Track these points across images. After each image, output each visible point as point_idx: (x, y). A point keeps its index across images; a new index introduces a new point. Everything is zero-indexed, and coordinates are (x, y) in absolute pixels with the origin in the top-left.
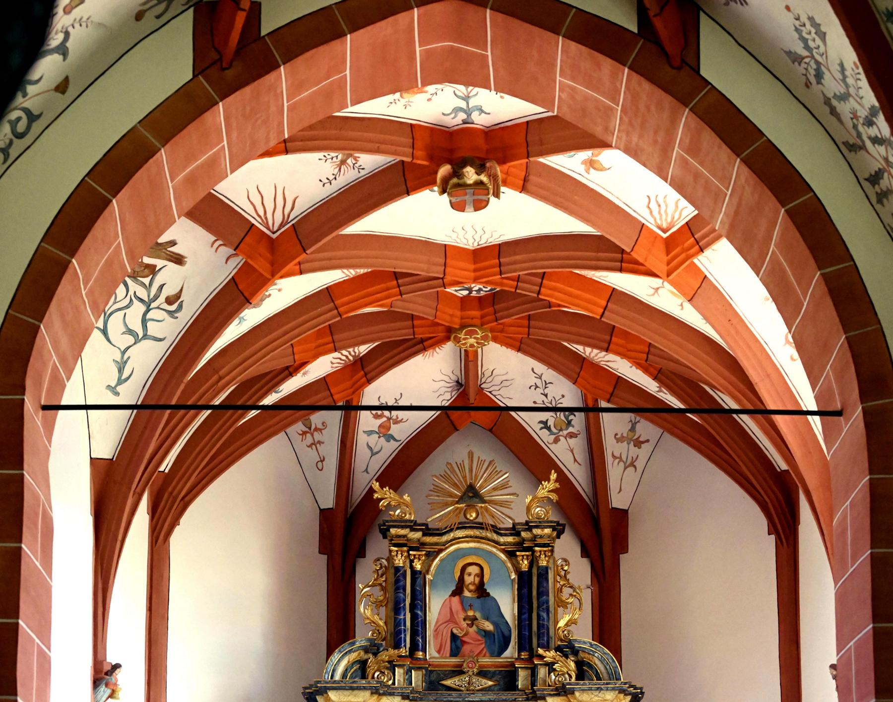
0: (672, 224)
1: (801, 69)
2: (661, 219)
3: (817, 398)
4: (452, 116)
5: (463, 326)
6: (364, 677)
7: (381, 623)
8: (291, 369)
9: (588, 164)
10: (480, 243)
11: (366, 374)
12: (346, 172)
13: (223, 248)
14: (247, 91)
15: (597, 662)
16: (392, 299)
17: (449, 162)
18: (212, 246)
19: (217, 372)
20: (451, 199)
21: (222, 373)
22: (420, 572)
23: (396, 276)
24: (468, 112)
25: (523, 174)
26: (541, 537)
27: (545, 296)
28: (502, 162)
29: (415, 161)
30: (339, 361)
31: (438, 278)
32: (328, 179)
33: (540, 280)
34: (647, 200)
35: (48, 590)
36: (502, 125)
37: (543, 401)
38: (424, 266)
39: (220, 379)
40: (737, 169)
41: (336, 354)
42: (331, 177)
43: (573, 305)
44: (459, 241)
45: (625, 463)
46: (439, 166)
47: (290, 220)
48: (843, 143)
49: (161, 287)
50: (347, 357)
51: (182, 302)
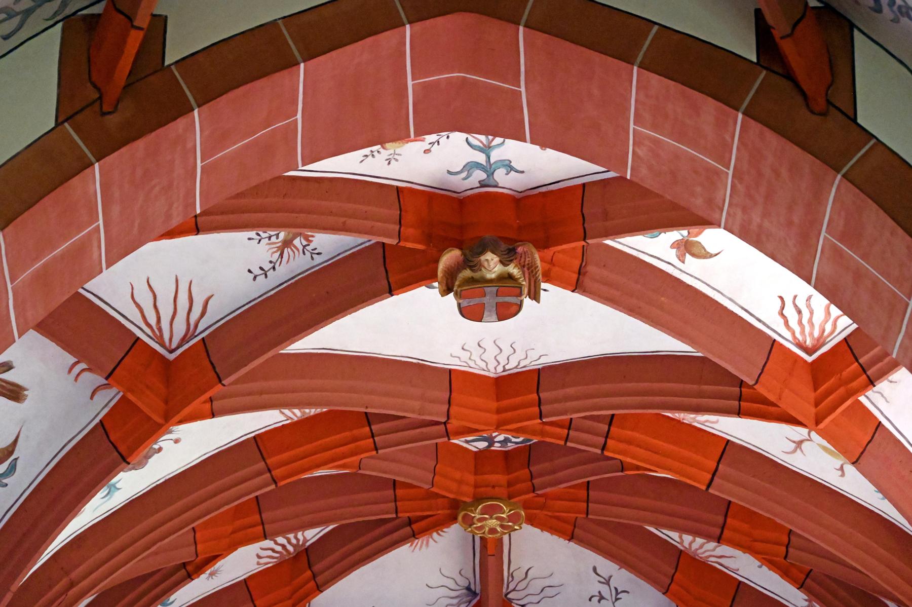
0: (821, 341)
4: (464, 175)
5: (478, 500)
8: (189, 568)
9: (682, 248)
11: (314, 576)
12: (291, 258)
13: (87, 375)
14: (140, 145)
16: (362, 456)
19: (67, 573)
20: (461, 301)
21: (74, 575)
23: (368, 419)
24: (489, 169)
25: (577, 263)
27: (613, 452)
28: (542, 245)
29: (402, 244)
30: (270, 553)
31: (437, 423)
32: (261, 268)
33: (606, 427)
34: (779, 302)
36: (544, 189)
38: (417, 404)
39: (72, 585)
41: (268, 543)
43: (658, 467)
44: (472, 364)
46: (441, 252)
47: (198, 332)
50: (283, 546)
51: (16, 459)
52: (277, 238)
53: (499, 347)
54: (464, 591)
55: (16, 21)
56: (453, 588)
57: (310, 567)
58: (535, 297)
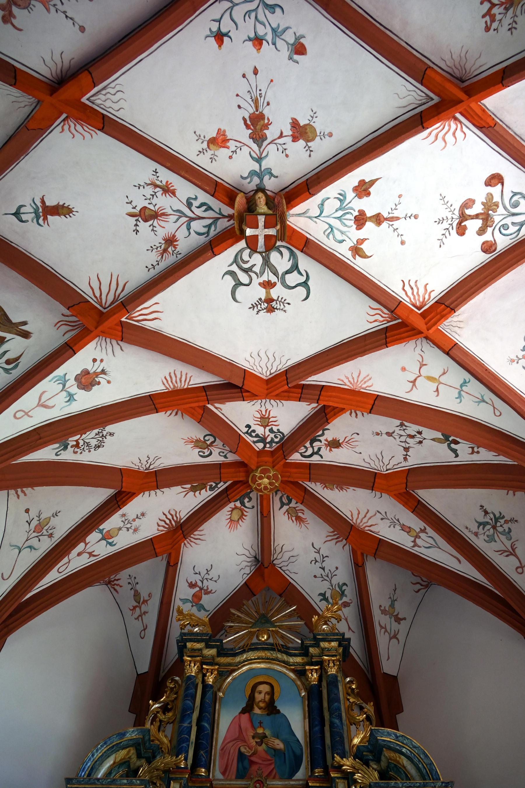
2: (414, 298)
4: (248, 180)
10: (272, 372)
12: (167, 258)
18: (55, 326)
22: (211, 686)
26: (329, 650)
32: (152, 265)
34: (402, 282)
37: (321, 574)
45: (390, 634)
47: (119, 299)
49: (5, 352)
51: (19, 362)
52: (161, 248)
53: (267, 356)
54: (253, 559)
56: (248, 556)
57: (181, 530)
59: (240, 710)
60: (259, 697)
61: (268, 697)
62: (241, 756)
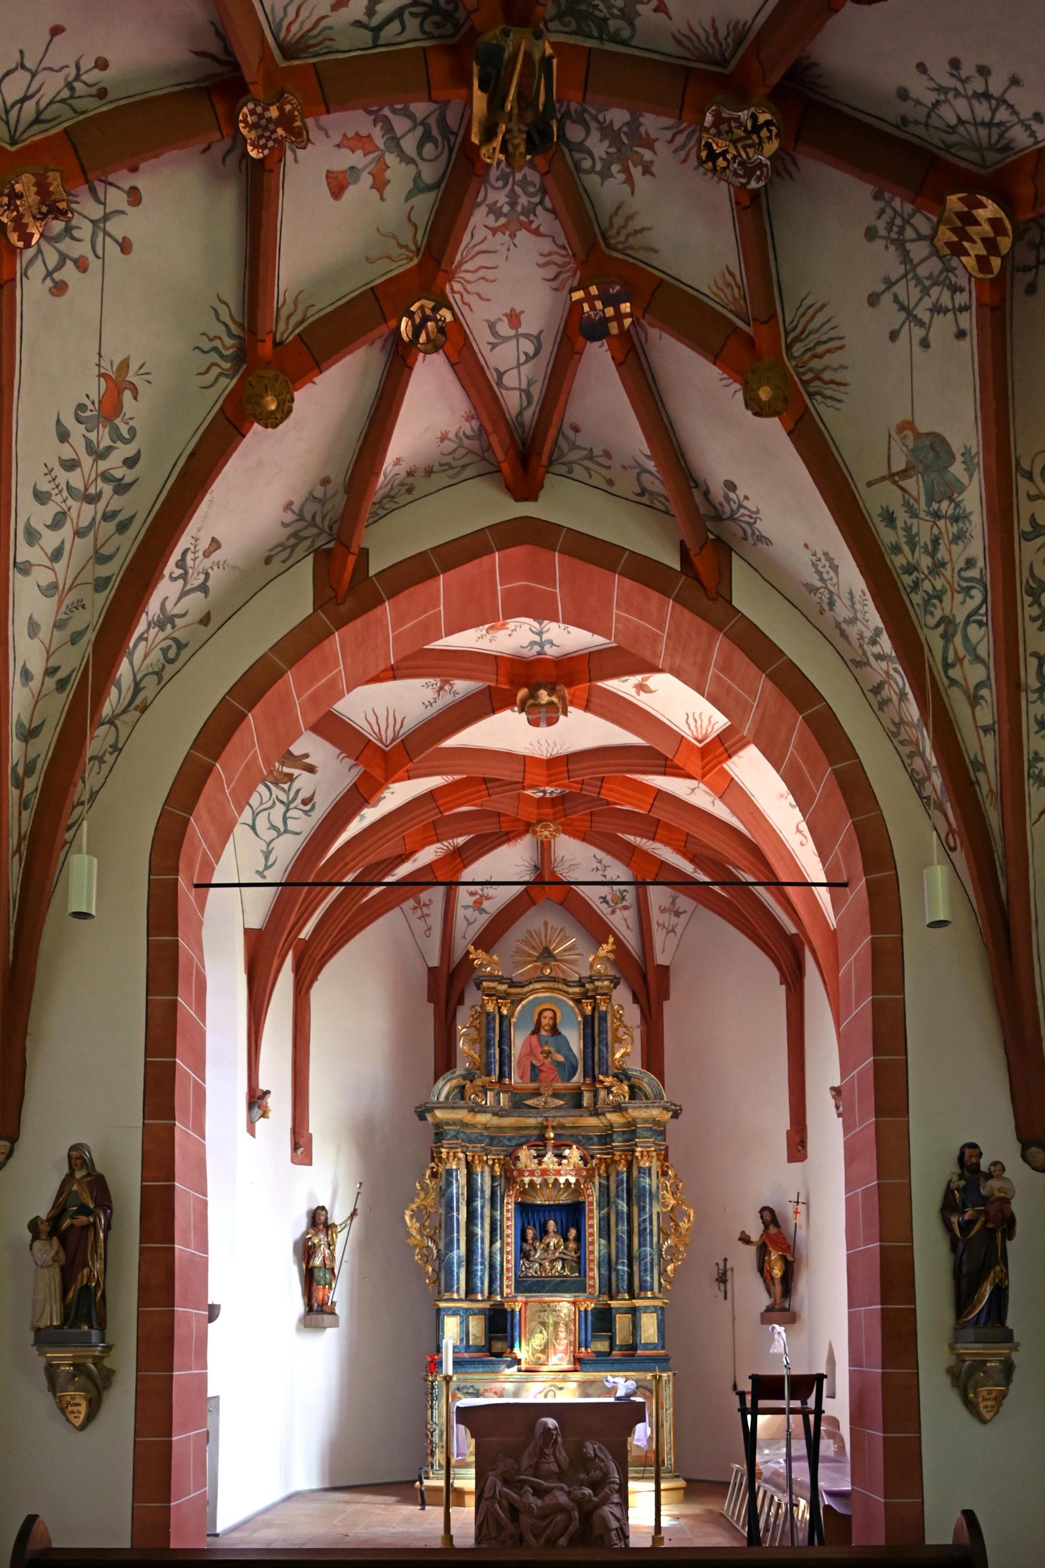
1: (816, 599)
3: (826, 873)
5: (539, 821)
6: (463, 1098)
7: (476, 1056)
15: (646, 1085)
17: (527, 686)
23: (485, 781)
35: (202, 1035)
40: (763, 682)
42: (432, 701)
48: (851, 661)
55: (288, 551)
58: (565, 713)
59: (530, 1032)
60: (544, 1022)
61: (551, 1022)
62: (533, 1066)
